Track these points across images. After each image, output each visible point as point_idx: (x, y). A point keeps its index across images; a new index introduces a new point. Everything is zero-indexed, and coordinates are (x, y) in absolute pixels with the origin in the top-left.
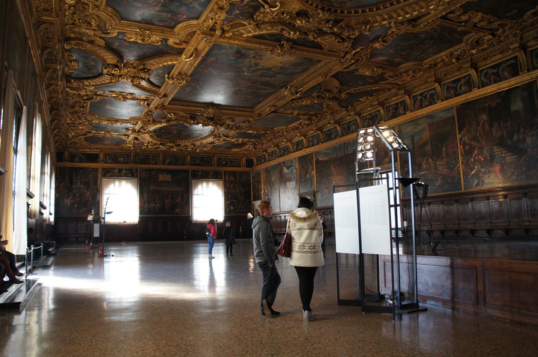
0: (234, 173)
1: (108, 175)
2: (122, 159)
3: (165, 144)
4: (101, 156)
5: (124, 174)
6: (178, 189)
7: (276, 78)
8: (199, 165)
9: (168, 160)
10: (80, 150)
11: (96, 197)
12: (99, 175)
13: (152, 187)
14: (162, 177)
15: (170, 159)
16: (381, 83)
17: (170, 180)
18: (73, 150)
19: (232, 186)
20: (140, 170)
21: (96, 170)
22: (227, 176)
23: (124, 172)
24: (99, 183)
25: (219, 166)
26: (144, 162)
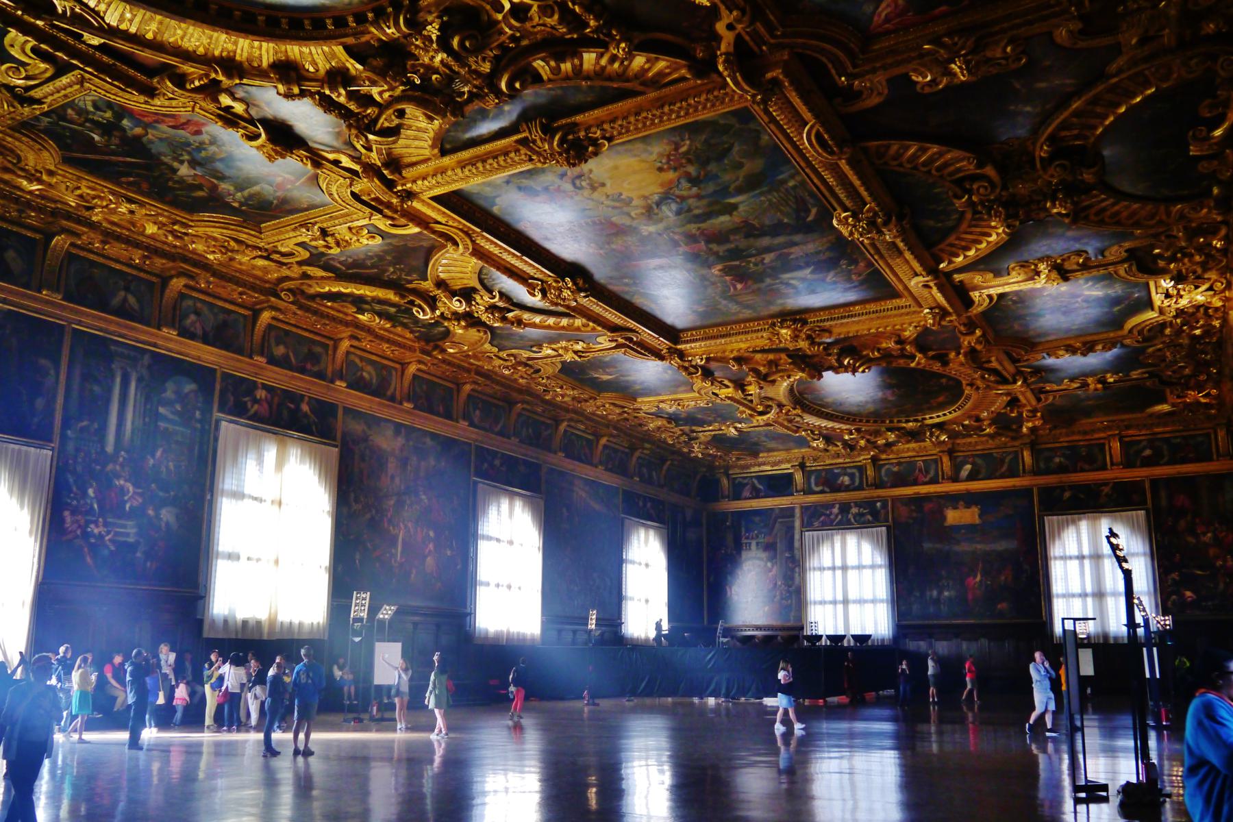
0: (1188, 482)
1: (816, 524)
2: (846, 480)
3: (899, 429)
4: (798, 477)
6: (1002, 546)
7: (741, 208)
8: (1062, 469)
9: (969, 467)
10: (753, 470)
11: (792, 578)
12: (797, 524)
13: (927, 546)
14: (953, 516)
15: (973, 464)
16: (1113, 67)
17: (977, 521)
18: (738, 471)
19: (1182, 524)
20: (893, 501)
21: (788, 513)
22: (1163, 494)
23: (854, 510)
24: (797, 544)
25: (1128, 463)
26: (901, 480)
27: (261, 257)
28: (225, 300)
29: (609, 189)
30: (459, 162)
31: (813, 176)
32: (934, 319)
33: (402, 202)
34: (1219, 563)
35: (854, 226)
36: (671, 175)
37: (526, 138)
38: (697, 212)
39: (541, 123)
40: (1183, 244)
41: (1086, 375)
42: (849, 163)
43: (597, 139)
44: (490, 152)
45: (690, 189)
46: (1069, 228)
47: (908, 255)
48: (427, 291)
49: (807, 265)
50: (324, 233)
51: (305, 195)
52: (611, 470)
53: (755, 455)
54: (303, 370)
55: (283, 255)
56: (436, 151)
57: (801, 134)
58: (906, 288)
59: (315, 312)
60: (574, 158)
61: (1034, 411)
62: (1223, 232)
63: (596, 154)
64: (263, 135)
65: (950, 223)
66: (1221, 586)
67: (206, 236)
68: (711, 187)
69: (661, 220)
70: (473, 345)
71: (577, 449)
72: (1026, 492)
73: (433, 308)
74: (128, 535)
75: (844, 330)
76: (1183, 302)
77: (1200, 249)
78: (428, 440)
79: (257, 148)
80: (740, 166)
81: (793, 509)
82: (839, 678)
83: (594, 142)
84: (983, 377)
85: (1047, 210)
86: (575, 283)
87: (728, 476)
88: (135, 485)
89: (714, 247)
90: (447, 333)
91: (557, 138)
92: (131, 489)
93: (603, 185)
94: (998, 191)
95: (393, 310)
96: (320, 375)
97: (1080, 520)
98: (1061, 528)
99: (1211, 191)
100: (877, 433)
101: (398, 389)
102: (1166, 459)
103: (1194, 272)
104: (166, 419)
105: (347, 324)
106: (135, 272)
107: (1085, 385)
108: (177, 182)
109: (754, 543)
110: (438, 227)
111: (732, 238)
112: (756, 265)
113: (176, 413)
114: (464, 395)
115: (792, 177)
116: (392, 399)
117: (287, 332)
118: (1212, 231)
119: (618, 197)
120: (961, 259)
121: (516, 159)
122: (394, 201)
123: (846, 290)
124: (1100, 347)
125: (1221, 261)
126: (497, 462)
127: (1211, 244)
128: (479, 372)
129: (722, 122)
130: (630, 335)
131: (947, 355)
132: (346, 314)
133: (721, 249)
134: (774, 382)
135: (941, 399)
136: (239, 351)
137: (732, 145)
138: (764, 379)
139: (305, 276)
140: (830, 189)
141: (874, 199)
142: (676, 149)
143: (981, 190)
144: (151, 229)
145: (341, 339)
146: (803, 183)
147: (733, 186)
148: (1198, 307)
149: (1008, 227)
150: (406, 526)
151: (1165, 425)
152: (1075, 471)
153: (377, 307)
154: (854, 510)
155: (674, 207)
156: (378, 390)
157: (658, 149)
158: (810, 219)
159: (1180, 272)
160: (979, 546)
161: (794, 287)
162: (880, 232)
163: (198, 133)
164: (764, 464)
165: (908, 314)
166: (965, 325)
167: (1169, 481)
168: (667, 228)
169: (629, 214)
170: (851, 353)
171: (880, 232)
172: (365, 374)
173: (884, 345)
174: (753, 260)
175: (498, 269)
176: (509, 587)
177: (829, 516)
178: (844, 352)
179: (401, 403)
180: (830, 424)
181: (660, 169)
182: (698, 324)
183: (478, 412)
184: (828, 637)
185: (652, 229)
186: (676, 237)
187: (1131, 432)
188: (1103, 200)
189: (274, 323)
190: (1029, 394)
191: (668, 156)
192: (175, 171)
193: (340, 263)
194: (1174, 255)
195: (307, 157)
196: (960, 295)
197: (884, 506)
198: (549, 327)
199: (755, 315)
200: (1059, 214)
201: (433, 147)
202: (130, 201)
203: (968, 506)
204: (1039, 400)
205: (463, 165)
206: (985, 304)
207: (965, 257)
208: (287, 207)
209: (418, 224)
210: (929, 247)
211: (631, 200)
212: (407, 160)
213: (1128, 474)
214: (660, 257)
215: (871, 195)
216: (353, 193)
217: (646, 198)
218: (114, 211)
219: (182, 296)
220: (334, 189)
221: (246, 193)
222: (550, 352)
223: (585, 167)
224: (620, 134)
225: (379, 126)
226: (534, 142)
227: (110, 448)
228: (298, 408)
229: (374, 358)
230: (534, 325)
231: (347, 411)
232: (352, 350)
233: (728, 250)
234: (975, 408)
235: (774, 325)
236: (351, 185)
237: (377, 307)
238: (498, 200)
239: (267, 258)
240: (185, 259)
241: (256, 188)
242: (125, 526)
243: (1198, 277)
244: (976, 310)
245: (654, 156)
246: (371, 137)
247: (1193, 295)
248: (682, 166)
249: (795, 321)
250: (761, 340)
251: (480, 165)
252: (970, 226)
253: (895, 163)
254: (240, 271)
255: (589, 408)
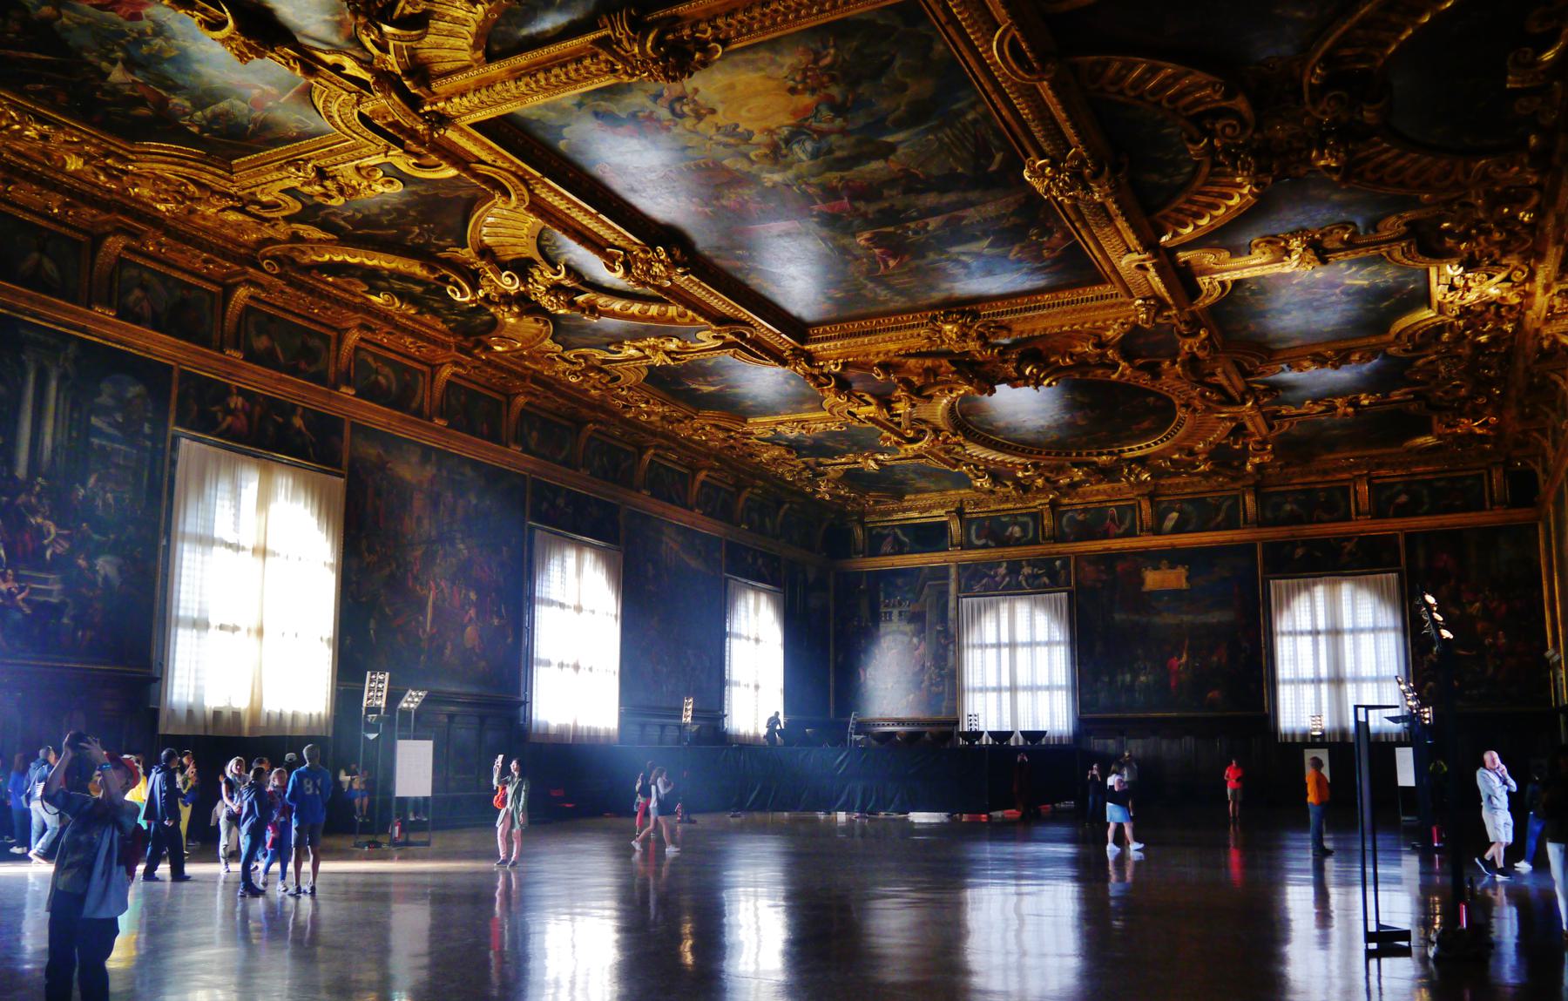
0: (1452, 538)
1: (977, 588)
2: (1017, 531)
3: (1087, 464)
4: (955, 526)
5: (1027, 578)
6: (1215, 617)
7: (901, 150)
8: (1294, 519)
9: (1175, 515)
10: (895, 517)
11: (945, 659)
12: (952, 587)
13: (1118, 617)
14: (1153, 579)
17: (1184, 585)
21: (941, 573)
23: (1027, 570)
24: (951, 614)
25: (1378, 512)
27: (233, 208)
28: (184, 271)
29: (720, 119)
30: (512, 71)
31: (1000, 105)
32: (1148, 314)
33: (432, 129)
34: (1488, 641)
35: (1053, 179)
36: (807, 100)
37: (608, 37)
38: (839, 154)
39: (628, 14)
40: (1481, 215)
41: (1335, 395)
42: (1052, 87)
43: (707, 42)
44: (556, 58)
45: (832, 120)
46: (1335, 187)
47: (1121, 223)
48: (466, 262)
49: (985, 235)
50: (322, 174)
51: (291, 115)
52: (709, 515)
53: (899, 497)
54: (294, 371)
55: (264, 206)
56: (479, 54)
57: (989, 42)
58: (1114, 270)
59: (312, 291)
60: (674, 70)
61: (1264, 442)
62: (1535, 199)
63: (705, 64)
64: (231, 22)
65: (1179, 179)
66: (1491, 670)
67: (155, 175)
68: (861, 119)
69: (789, 166)
70: (527, 342)
71: (668, 486)
72: (1247, 549)
73: (475, 289)
74: (49, 593)
75: (1028, 327)
76: (1471, 297)
77: (1502, 224)
78: (469, 472)
79: (224, 41)
80: (903, 88)
81: (946, 569)
82: (1351, 794)
83: (703, 46)
84: (1202, 395)
85: (1308, 161)
86: (669, 255)
87: (863, 524)
88: (57, 525)
89: (861, 205)
90: (494, 324)
91: (651, 37)
92: (53, 530)
93: (713, 111)
94: (1250, 132)
95: (419, 289)
96: (320, 378)
97: (1315, 584)
98: (1291, 594)
99: (1527, 141)
100: (1060, 470)
101: (427, 400)
102: (1425, 508)
103: (1490, 256)
104: (100, 433)
105: (355, 308)
106: (52, 226)
107: (1332, 408)
108: (106, 93)
109: (895, 612)
110: (483, 169)
111: (886, 192)
112: (916, 232)
113: (116, 425)
114: (515, 411)
115: (973, 106)
116: (419, 413)
117: (271, 318)
118: (1519, 200)
119: (732, 131)
120: (1189, 230)
121: (593, 68)
122: (420, 127)
123: (1034, 271)
124: (1356, 357)
125: (1525, 242)
126: (561, 502)
127: (1516, 217)
128: (537, 378)
129: (881, 22)
130: (742, 329)
131: (1159, 364)
132: (354, 295)
133: (871, 209)
134: (930, 397)
135: (1146, 425)
136: (205, 343)
137: (893, 57)
138: (919, 393)
139: (296, 238)
140: (1024, 124)
141: (1083, 141)
142: (816, 61)
143: (1228, 130)
144: (74, 164)
145: (347, 330)
146: (987, 116)
147: (891, 118)
148: (1488, 304)
149: (1257, 185)
150: (437, 585)
151: (1427, 464)
152: (1310, 522)
153: (397, 285)
154: (1027, 570)
155: (809, 146)
156: (400, 400)
157: (790, 60)
158: (993, 168)
159: (1472, 254)
160: (1187, 618)
161: (966, 266)
162: (1087, 188)
163: (136, 17)
164: (911, 509)
165: (1112, 306)
166: (1187, 323)
167: (1429, 536)
168: (798, 177)
169: (747, 156)
170: (1033, 360)
171: (1087, 188)
172: (382, 379)
173: (1079, 349)
174: (912, 225)
175: (565, 232)
176: (577, 667)
177: (993, 577)
178: (1024, 360)
179: (431, 420)
180: (1000, 457)
181: (793, 91)
182: (833, 315)
183: (534, 434)
184: (990, 733)
185: (777, 177)
186: (811, 190)
187: (1383, 472)
188: (1387, 150)
189: (253, 304)
190: (1259, 420)
191: (806, 69)
192: (105, 75)
193: (345, 219)
194: (1468, 230)
195: (295, 59)
196: (1183, 280)
197: (1065, 565)
198: (633, 317)
199: (909, 304)
200: (1327, 167)
201: (475, 47)
202: (42, 120)
203: (1172, 566)
204: (1271, 427)
205: (516, 75)
206: (1216, 295)
207: (1196, 226)
208: (270, 136)
209: (454, 164)
210: (1149, 215)
211: (750, 134)
212: (438, 68)
213: (1377, 527)
214: (788, 219)
215: (1078, 134)
216: (360, 115)
217: (771, 132)
218: (18, 135)
219: (121, 262)
220: (334, 109)
221: (208, 112)
222: (633, 352)
223: (689, 84)
224: (739, 34)
225: (398, 12)
226: (619, 42)
227: (21, 471)
228: (288, 425)
229: (392, 356)
230: (613, 314)
231: (358, 428)
232: (363, 344)
233: (880, 211)
234: (1189, 436)
235: (935, 318)
236: (358, 103)
237: (397, 285)
238: (566, 132)
239: (242, 210)
240: (125, 210)
241: (224, 105)
242: (45, 581)
243: (1494, 263)
244: (1203, 302)
245: (785, 71)
246: (387, 29)
247: (1484, 287)
248: (823, 85)
249: (963, 314)
250: (917, 339)
251: (541, 76)
252: (1205, 184)
253: (1113, 89)
254: (205, 229)
255: (684, 431)
